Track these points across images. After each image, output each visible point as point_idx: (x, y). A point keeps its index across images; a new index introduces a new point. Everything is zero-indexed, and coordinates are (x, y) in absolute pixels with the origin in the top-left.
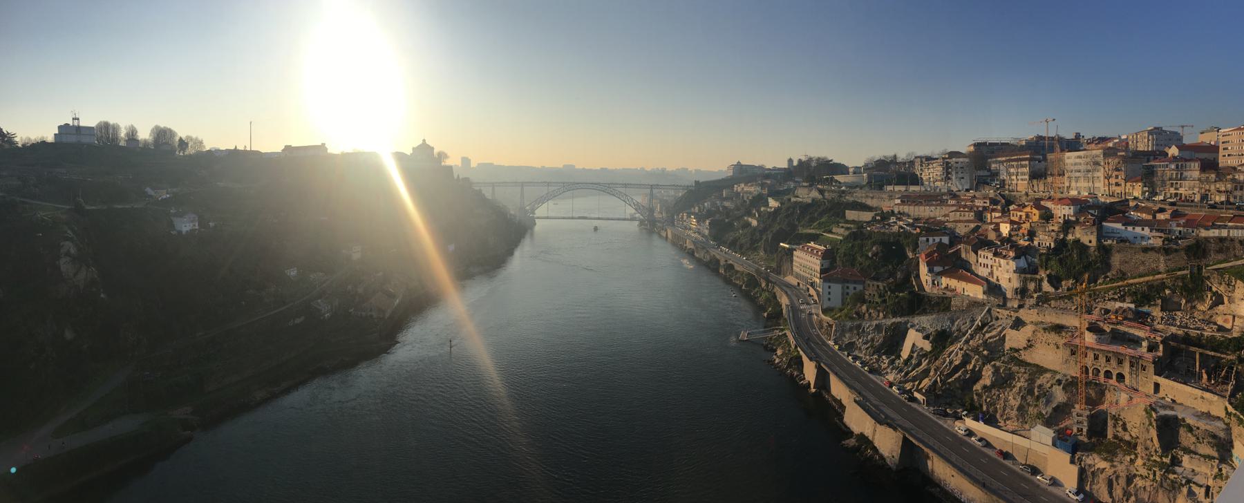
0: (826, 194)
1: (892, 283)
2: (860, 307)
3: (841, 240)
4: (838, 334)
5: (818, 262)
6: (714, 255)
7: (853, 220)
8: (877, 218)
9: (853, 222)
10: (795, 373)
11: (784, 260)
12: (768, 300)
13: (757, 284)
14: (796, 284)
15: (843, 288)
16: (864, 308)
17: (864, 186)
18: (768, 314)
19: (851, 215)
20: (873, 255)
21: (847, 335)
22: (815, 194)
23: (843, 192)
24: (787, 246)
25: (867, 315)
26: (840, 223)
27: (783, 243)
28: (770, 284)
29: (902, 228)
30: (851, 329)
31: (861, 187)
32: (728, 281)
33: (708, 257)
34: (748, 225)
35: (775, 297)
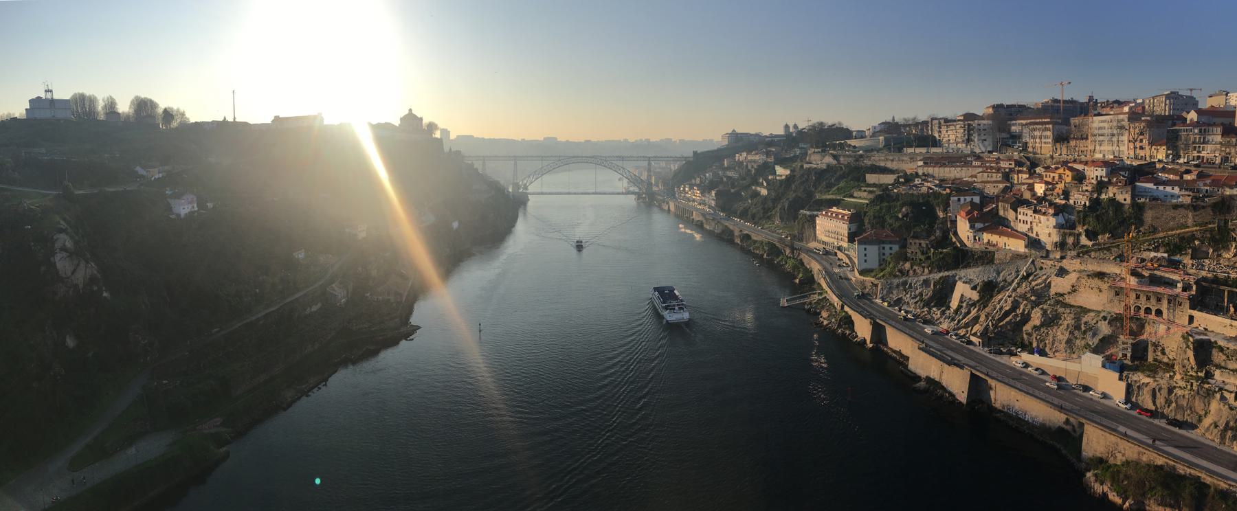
1: (934, 240)
3: (867, 204)
4: (885, 292)
5: (846, 226)
7: (874, 184)
8: (901, 180)
9: (874, 185)
11: (806, 227)
12: (795, 267)
15: (879, 249)
17: (881, 149)
19: (871, 178)
20: (903, 217)
21: (895, 292)
23: (861, 156)
24: (808, 213)
25: (911, 272)
26: (863, 187)
29: (931, 189)
30: (898, 286)
31: (878, 150)
35: (802, 264)
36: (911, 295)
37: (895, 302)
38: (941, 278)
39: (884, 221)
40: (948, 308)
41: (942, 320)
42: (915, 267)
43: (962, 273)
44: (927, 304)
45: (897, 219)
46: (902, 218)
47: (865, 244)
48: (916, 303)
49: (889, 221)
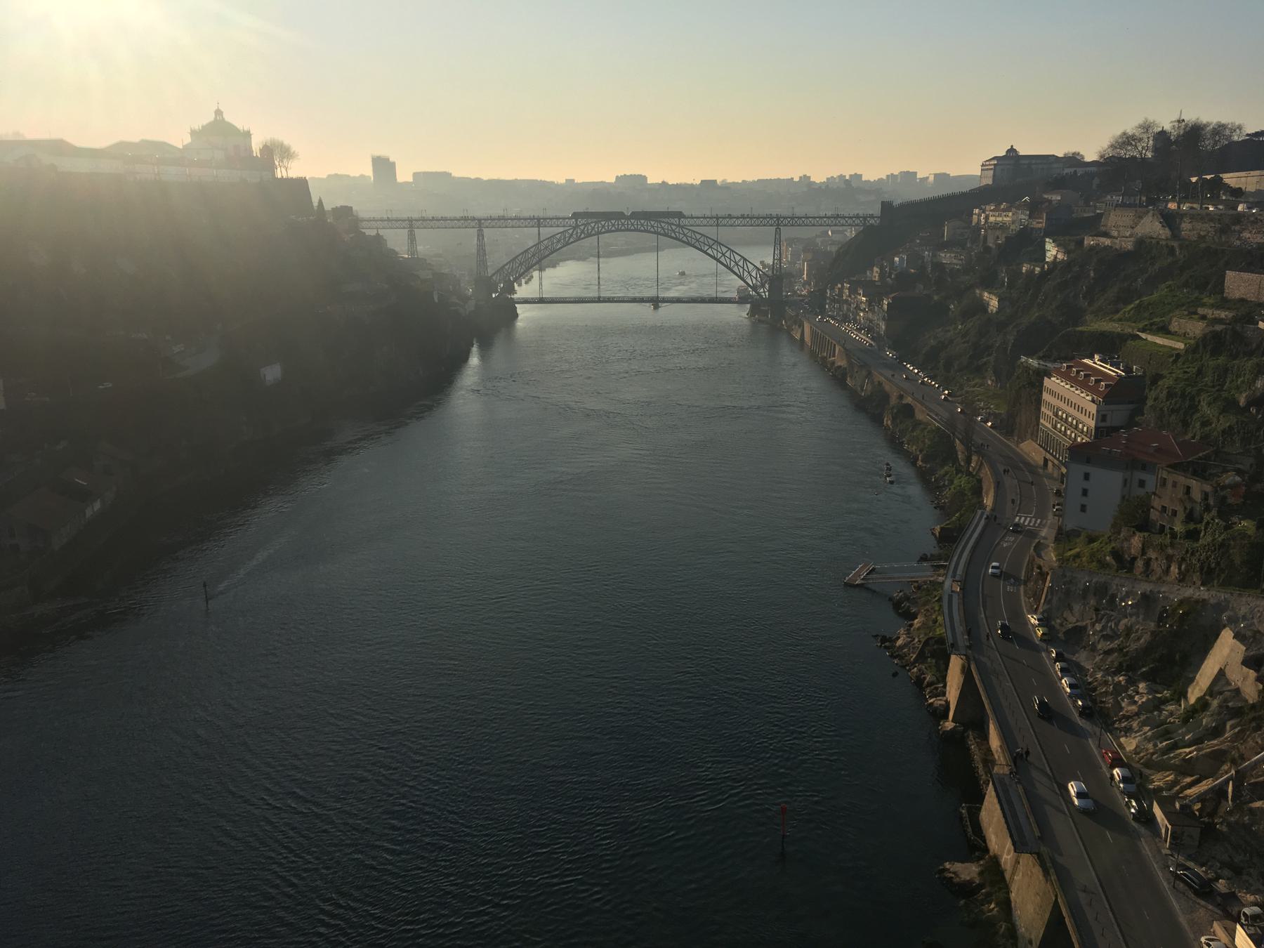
0: (1186, 226)
1: (1234, 486)
2: (1127, 539)
5: (1093, 408)
6: (880, 384)
10: (928, 678)
13: (951, 456)
14: (1042, 463)
15: (1125, 481)
16: (1136, 541)
18: (942, 529)
20: (1250, 403)
21: (1077, 607)
22: (1151, 226)
23: (1239, 218)
26: (1203, 305)
27: (1030, 354)
28: (974, 458)
32: (895, 444)
33: (870, 388)
34: (983, 307)
35: (978, 491)
36: (1104, 628)
37: (1067, 633)
38: (1181, 602)
39: (1194, 408)
40: (1183, 694)
41: (1135, 725)
42: (1152, 554)
43: (1246, 604)
44: (1130, 666)
45: (1230, 405)
46: (1247, 408)
47: (1088, 461)
48: (1108, 653)
49: (1206, 410)
